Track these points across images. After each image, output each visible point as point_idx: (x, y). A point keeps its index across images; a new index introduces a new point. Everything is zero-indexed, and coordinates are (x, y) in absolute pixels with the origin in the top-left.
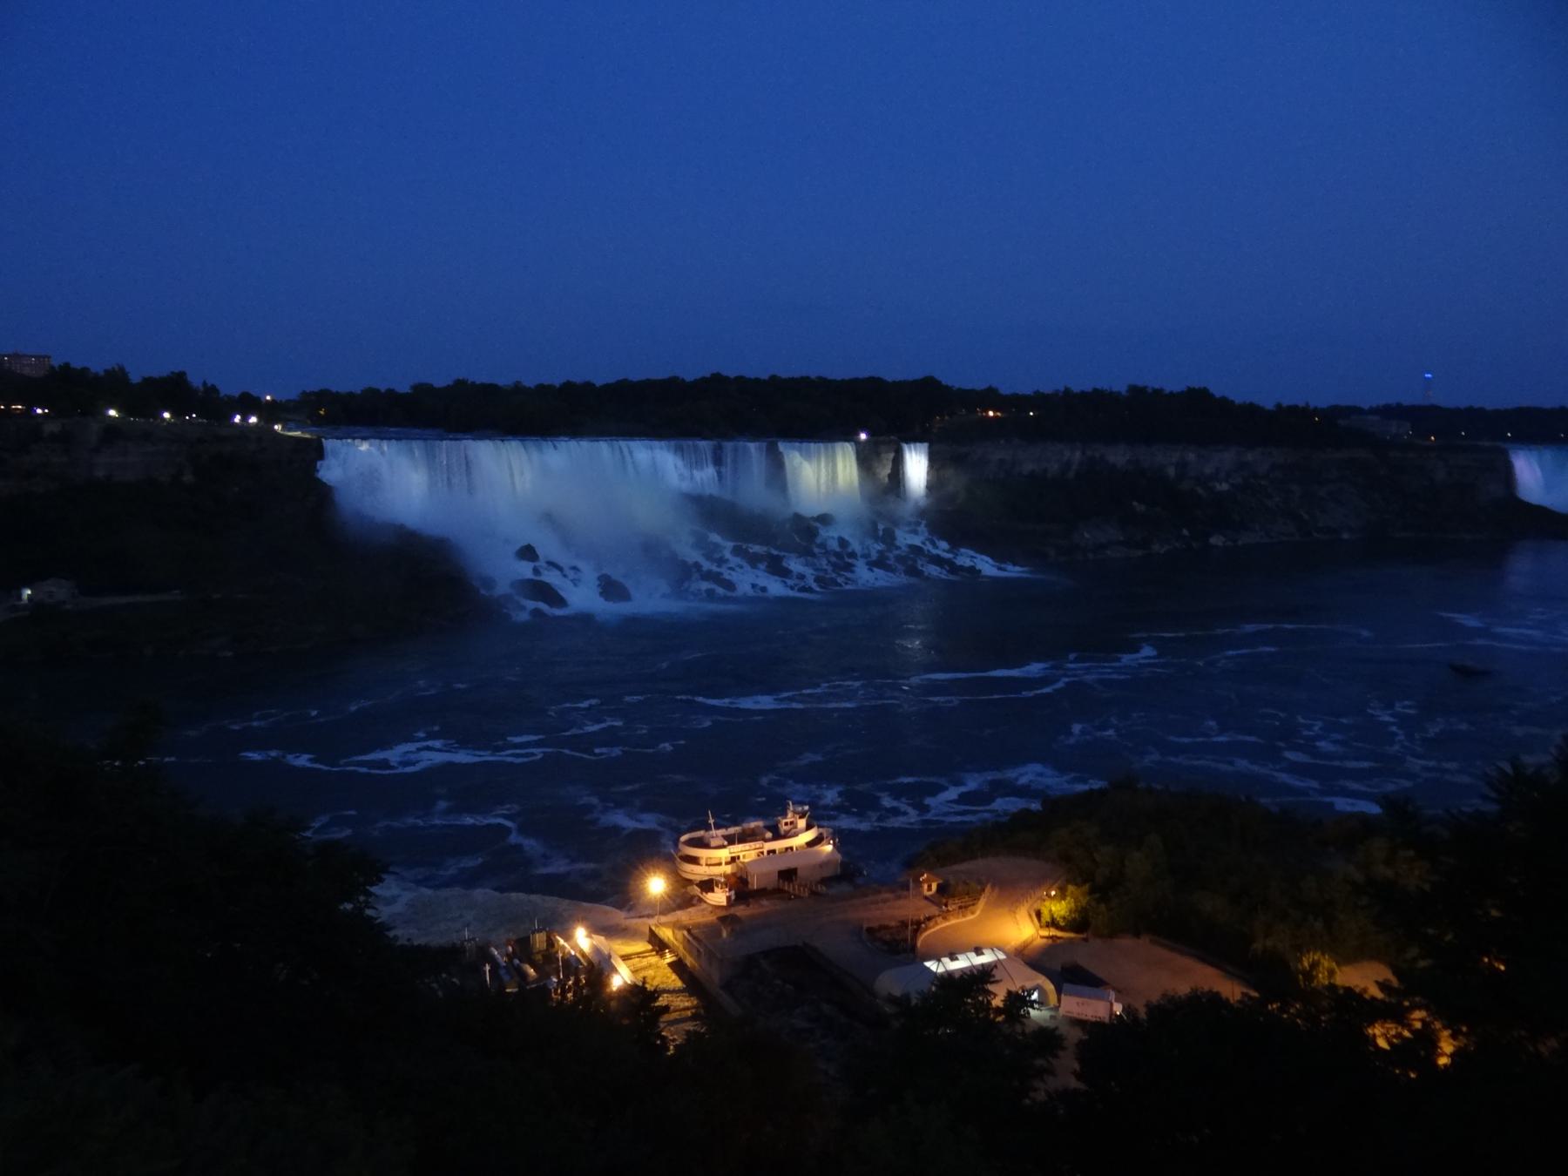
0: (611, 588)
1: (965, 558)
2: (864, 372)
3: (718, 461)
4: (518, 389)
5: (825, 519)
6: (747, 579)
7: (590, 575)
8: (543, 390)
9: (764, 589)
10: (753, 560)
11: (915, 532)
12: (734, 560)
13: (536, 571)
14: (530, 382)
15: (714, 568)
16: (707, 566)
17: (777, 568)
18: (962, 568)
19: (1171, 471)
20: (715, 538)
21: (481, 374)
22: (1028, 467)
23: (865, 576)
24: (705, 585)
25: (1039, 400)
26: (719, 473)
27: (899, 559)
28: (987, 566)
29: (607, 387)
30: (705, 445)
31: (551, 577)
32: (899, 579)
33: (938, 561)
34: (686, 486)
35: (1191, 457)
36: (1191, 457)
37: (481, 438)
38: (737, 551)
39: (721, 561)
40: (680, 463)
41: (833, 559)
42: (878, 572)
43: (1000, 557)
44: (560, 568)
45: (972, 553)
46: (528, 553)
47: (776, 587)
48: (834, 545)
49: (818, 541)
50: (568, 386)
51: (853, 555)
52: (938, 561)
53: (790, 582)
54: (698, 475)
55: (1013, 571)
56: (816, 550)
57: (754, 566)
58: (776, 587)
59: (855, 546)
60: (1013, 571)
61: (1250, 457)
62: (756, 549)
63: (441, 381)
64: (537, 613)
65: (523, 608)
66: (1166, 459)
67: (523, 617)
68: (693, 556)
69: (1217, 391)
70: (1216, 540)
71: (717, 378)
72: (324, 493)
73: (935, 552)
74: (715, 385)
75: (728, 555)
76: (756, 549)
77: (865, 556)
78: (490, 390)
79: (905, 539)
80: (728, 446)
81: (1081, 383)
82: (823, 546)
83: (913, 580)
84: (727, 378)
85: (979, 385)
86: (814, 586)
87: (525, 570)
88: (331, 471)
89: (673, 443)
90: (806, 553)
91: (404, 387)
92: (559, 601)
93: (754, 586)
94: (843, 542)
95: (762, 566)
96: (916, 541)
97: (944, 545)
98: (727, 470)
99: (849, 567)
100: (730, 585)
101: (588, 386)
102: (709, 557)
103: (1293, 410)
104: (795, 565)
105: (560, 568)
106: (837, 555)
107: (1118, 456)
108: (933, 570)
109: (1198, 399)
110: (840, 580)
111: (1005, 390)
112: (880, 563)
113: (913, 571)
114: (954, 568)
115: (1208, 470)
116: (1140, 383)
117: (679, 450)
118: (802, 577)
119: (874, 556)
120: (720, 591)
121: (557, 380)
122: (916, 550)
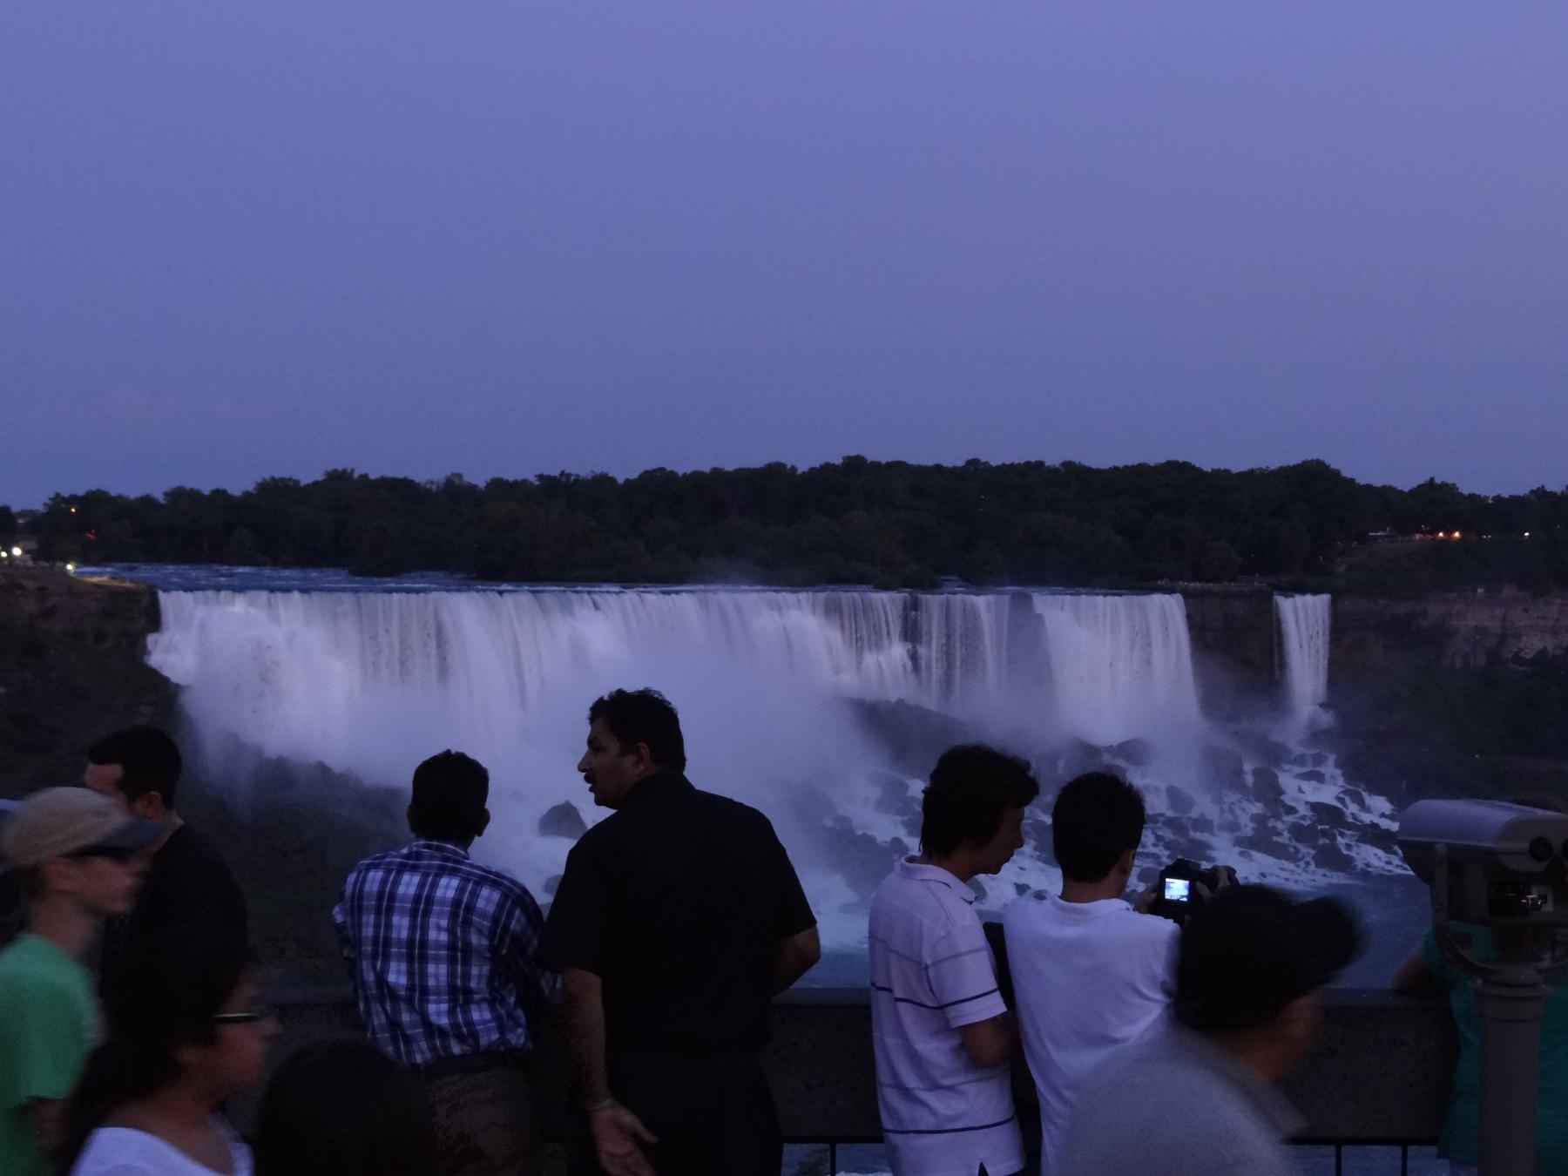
3: (911, 633)
22: (1533, 644)
26: (914, 657)
27: (1298, 832)
30: (888, 602)
33: (1374, 836)
34: (849, 681)
40: (835, 636)
41: (1168, 834)
51: (1203, 824)
52: (1374, 836)
54: (870, 659)
59: (1204, 806)
73: (1367, 818)
83: (1338, 878)
89: (822, 596)
94: (1175, 796)
96: (1327, 794)
97: (1380, 804)
106: (1171, 823)
108: (1372, 857)
112: (1261, 841)
113: (1332, 859)
117: (833, 610)
119: (1248, 829)
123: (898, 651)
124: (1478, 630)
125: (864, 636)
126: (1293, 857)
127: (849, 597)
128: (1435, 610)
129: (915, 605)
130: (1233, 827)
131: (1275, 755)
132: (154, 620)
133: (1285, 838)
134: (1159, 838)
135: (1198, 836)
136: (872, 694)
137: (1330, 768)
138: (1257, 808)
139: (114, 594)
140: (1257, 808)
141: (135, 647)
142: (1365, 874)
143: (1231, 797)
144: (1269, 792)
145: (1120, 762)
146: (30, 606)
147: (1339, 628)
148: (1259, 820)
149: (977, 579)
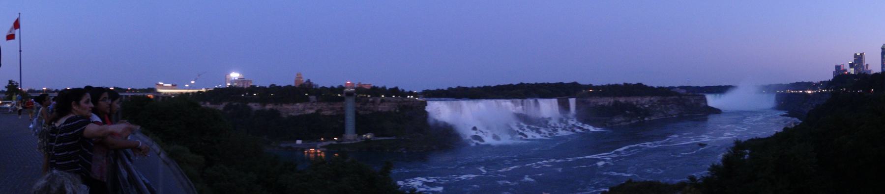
0: (495, 137)
1: (586, 127)
2: (558, 81)
3: (522, 104)
4: (473, 88)
5: (550, 118)
6: (531, 135)
7: (490, 135)
8: (479, 88)
9: (535, 137)
10: (532, 129)
11: (572, 121)
12: (527, 130)
13: (476, 133)
14: (476, 86)
15: (522, 132)
16: (520, 131)
17: (538, 132)
18: (585, 129)
19: (635, 103)
20: (522, 124)
21: (463, 85)
22: (600, 103)
23: (561, 133)
24: (520, 136)
25: (603, 87)
26: (523, 108)
27: (570, 128)
28: (592, 129)
29: (495, 87)
30: (519, 101)
31: (480, 134)
32: (571, 133)
33: (579, 128)
34: (514, 111)
35: (639, 99)
36: (639, 99)
37: (464, 100)
38: (528, 127)
39: (524, 130)
41: (553, 128)
42: (564, 131)
43: (595, 126)
44: (483, 132)
45: (588, 125)
46: (475, 128)
47: (538, 136)
48: (553, 125)
49: (549, 124)
50: (485, 87)
51: (558, 127)
52: (579, 128)
53: (542, 135)
54: (517, 108)
55: (598, 130)
56: (549, 126)
57: (532, 131)
58: (538, 136)
59: (558, 125)
60: (598, 130)
61: (652, 99)
62: (533, 126)
63: (454, 86)
64: (477, 144)
65: (473, 143)
66: (634, 100)
67: (473, 145)
68: (517, 129)
69: (644, 84)
70: (646, 119)
71: (522, 84)
72: (426, 113)
73: (578, 125)
74: (521, 86)
75: (525, 128)
76: (533, 126)
77: (561, 127)
78: (466, 88)
79: (571, 122)
80: (525, 101)
81: (612, 82)
82: (550, 125)
83: (573, 133)
84: (524, 84)
85: (588, 84)
86: (548, 135)
87: (474, 133)
88: (428, 109)
90: (546, 127)
91: (445, 88)
92: (483, 141)
93: (532, 136)
94: (555, 124)
95: (534, 131)
96: (573, 123)
97: (580, 124)
98: (525, 107)
99: (556, 130)
100: (526, 136)
101: (490, 87)
102: (520, 129)
103: (661, 87)
104: (543, 130)
105: (483, 132)
106: (554, 127)
107: (622, 100)
108: (578, 130)
109: (640, 85)
110: (555, 134)
111: (594, 85)
112: (564, 129)
113: (573, 131)
114: (584, 130)
115: (643, 102)
116: (626, 82)
117: (512, 102)
118: (544, 133)
120: (524, 138)
121: (482, 86)
122: (574, 125)
123: (521, 107)
124: (594, 102)
125: (516, 105)
126: (568, 131)
127: (514, 100)
128: (588, 100)
129: (523, 101)
130: (561, 127)
131: (568, 118)
132: (426, 105)
133: (567, 129)
134: (552, 130)
135: (557, 129)
136: (517, 112)
137: (575, 120)
138: (565, 125)
139: (422, 102)
140: (565, 125)
141: (424, 108)
142: (577, 133)
143: (562, 124)
144: (566, 123)
145: (548, 120)
146: (411, 103)
147: (577, 103)
148: (565, 126)
149: (532, 97)
